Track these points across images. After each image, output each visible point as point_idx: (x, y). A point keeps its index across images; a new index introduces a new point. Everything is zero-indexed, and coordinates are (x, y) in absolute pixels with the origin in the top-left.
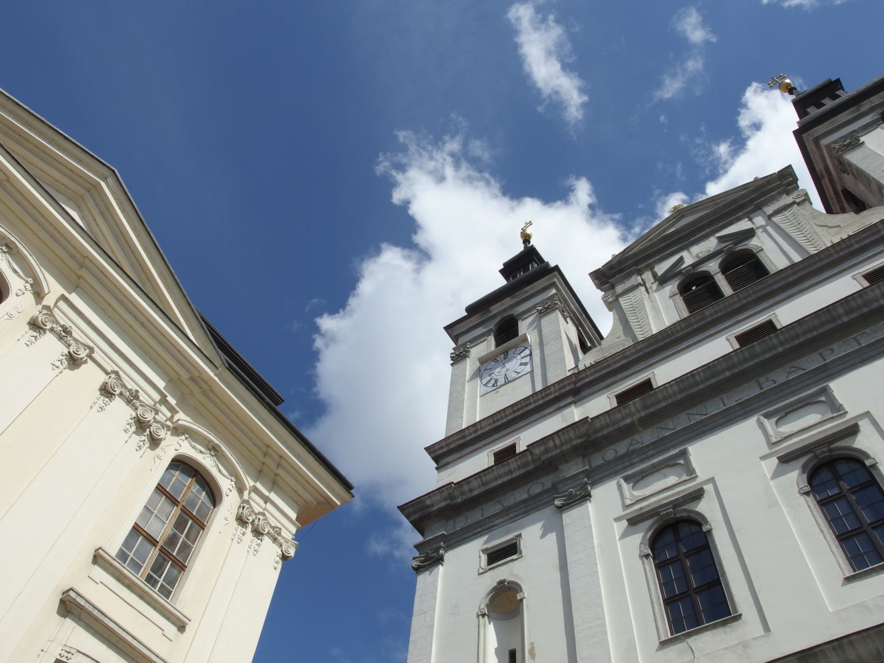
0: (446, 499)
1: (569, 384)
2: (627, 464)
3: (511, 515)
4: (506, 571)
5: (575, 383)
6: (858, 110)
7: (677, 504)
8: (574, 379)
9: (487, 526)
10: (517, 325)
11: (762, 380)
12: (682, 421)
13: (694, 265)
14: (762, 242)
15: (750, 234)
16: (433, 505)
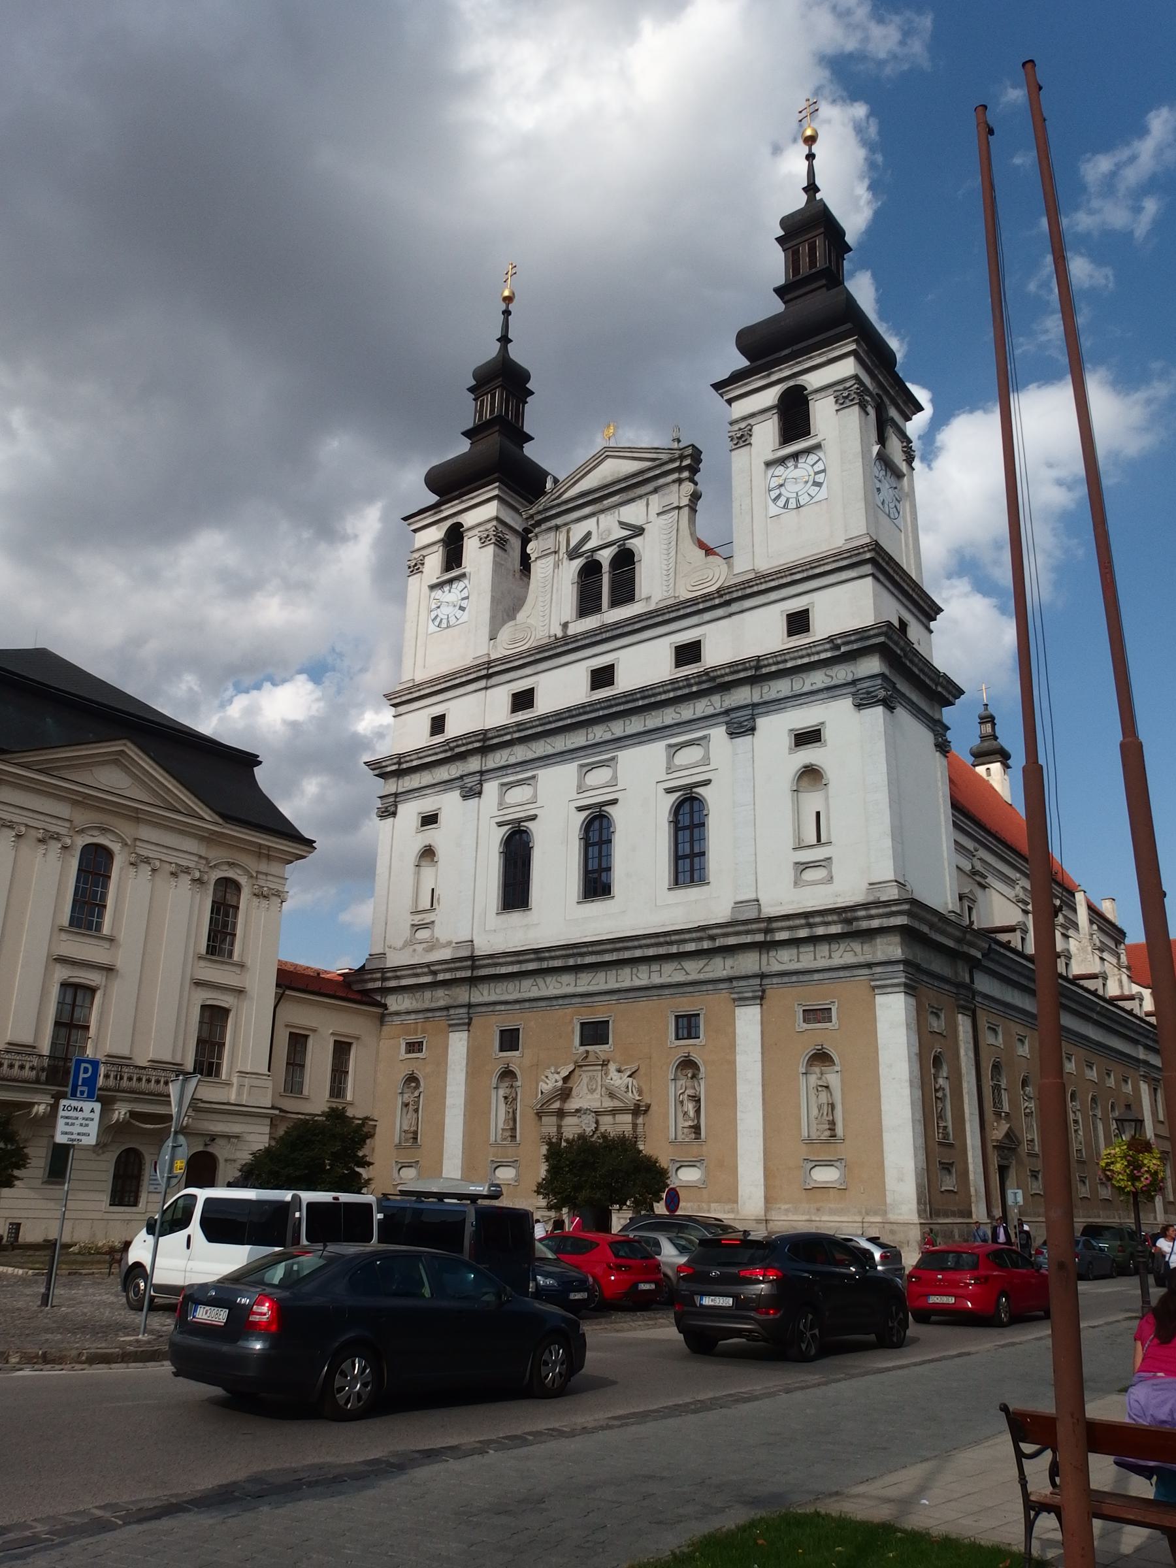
0: (395, 764)
1: (484, 669)
2: (504, 773)
3: (437, 789)
4: (432, 836)
5: (488, 669)
6: (769, 375)
7: (519, 821)
8: (486, 666)
9: (421, 794)
10: (462, 539)
11: (590, 730)
12: (541, 748)
13: (594, 550)
14: (644, 548)
15: (639, 531)
16: (386, 766)
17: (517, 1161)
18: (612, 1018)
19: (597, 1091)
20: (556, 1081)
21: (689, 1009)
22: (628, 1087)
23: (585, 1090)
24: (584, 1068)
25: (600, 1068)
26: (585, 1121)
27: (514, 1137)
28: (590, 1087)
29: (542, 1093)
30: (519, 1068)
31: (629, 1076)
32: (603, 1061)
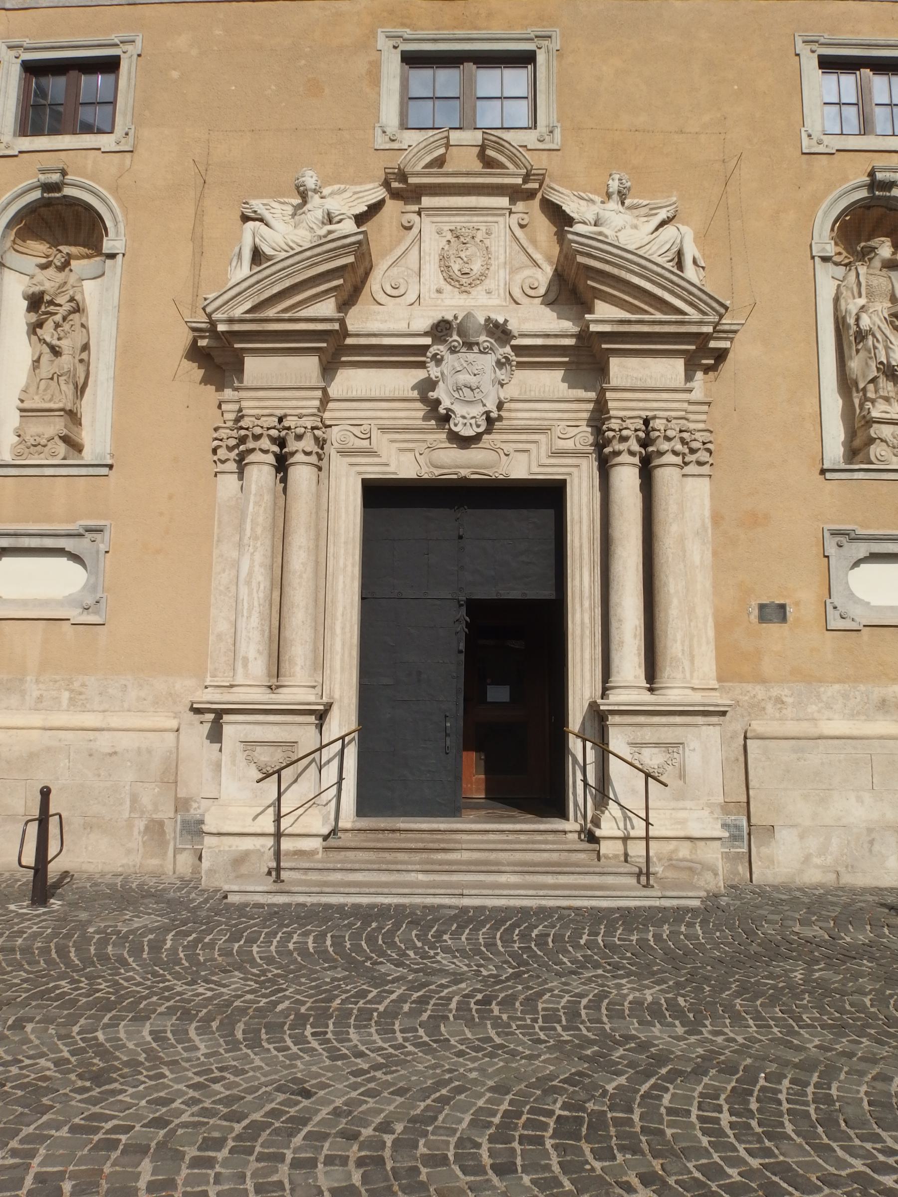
17: (99, 530)
18: (556, 44)
19: (490, 283)
20: (330, 219)
21: (881, 38)
22: (679, 260)
23: (432, 275)
24: (427, 201)
25: (503, 202)
26: (464, 378)
27: (74, 445)
28: (456, 267)
29: (258, 256)
30: (115, 190)
31: (663, 224)
32: (527, 178)
